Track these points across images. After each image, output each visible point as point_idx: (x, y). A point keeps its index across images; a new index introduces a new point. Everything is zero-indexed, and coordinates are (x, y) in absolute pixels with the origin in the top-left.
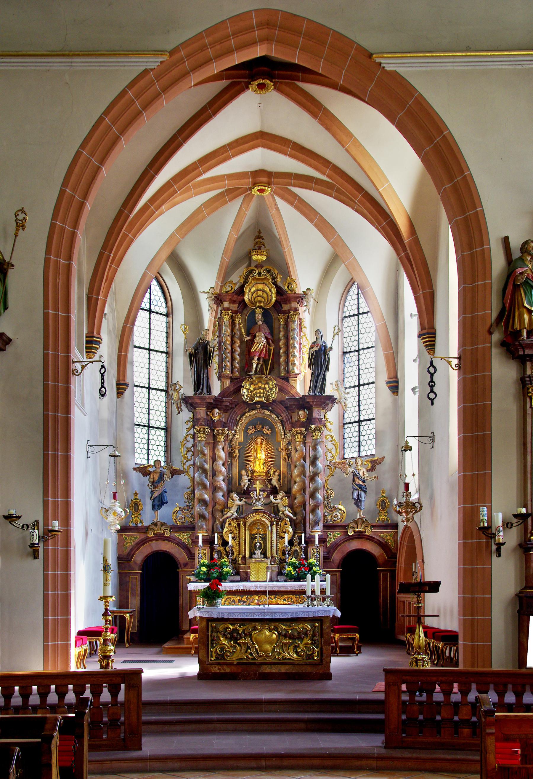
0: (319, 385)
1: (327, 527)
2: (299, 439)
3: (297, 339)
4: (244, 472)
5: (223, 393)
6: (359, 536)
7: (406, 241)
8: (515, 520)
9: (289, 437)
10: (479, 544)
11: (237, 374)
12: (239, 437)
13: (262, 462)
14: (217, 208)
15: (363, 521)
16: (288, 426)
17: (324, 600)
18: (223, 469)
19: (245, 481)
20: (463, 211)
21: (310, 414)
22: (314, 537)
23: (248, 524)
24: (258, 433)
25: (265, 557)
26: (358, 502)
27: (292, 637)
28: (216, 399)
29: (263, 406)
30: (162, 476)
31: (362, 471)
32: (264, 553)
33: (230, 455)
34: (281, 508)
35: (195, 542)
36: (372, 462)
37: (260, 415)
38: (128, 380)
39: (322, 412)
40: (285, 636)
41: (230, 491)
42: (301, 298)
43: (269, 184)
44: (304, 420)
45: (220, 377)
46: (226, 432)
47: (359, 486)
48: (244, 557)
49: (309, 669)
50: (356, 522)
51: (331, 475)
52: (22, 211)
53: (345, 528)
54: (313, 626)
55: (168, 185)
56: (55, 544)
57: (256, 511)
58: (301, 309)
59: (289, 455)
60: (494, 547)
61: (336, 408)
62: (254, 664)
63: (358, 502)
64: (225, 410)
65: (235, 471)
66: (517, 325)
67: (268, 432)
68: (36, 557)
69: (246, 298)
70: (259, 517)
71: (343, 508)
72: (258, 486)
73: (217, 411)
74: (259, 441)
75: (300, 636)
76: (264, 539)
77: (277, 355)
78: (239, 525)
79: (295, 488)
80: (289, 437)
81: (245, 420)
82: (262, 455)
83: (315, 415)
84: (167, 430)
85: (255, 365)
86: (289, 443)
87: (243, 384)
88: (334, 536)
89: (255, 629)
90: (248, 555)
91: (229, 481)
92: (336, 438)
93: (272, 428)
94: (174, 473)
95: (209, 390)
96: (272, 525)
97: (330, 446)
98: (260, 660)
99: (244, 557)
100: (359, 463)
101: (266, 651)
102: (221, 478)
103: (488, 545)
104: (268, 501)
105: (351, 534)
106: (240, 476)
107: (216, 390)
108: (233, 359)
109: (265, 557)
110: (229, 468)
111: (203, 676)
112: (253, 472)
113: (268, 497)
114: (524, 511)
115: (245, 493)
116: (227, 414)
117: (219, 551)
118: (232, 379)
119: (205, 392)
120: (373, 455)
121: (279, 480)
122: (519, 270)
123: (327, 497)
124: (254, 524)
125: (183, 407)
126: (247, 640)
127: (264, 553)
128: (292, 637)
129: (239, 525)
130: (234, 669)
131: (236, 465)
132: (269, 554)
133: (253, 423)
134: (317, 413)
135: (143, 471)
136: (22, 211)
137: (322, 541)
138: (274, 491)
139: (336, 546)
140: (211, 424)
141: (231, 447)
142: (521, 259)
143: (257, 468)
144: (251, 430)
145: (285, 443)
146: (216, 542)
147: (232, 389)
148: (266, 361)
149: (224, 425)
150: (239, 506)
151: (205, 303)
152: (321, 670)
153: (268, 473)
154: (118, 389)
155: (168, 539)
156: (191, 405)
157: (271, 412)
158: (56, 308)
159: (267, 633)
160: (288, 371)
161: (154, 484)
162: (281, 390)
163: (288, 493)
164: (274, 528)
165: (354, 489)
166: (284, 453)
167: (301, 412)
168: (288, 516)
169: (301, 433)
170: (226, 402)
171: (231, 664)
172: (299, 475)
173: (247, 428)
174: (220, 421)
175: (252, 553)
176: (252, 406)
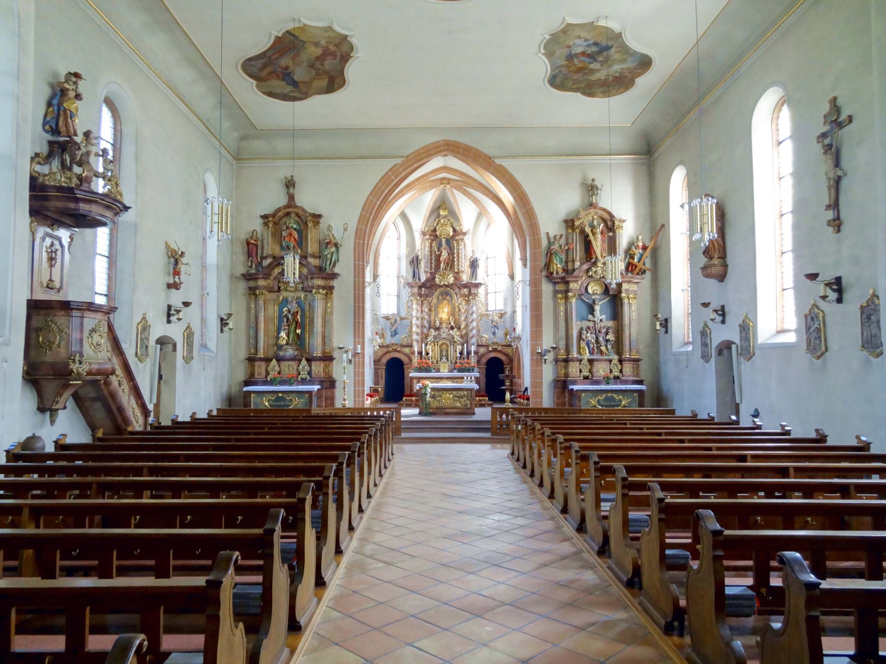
0: (474, 276)
1: (479, 346)
2: (464, 302)
3: (463, 253)
4: (437, 319)
5: (427, 280)
6: (495, 350)
7: (512, 218)
8: (551, 350)
9: (459, 301)
10: (537, 359)
11: (433, 271)
12: (435, 301)
13: (446, 313)
14: (423, 193)
15: (496, 343)
16: (459, 296)
17: (471, 382)
18: (427, 317)
19: (438, 324)
20: (530, 221)
21: (470, 291)
22: (471, 351)
23: (439, 345)
24: (444, 299)
25: (448, 360)
26: (494, 334)
27: (458, 397)
28: (423, 283)
29: (447, 286)
30: (396, 321)
31: (496, 318)
32: (447, 359)
33: (430, 310)
34: (455, 337)
35: (413, 353)
36: (501, 314)
37: (445, 290)
38: (378, 274)
39: (476, 290)
40: (456, 397)
41: (430, 328)
42: (465, 234)
43: (449, 183)
44: (467, 293)
45: (426, 272)
46: (428, 299)
47: (495, 325)
48: (437, 361)
49: (465, 411)
50: (493, 343)
51: (481, 320)
52: (346, 224)
53: (487, 346)
54: (468, 393)
55: (401, 191)
56: (359, 358)
57: (443, 339)
58: (465, 238)
59: (460, 310)
60: (543, 361)
61: (483, 287)
62: (442, 408)
63: (494, 334)
64: (427, 288)
65: (432, 317)
66: (551, 270)
67: (449, 299)
68: (351, 364)
69: (438, 233)
70: (444, 342)
71: (487, 337)
72: (444, 326)
73: (423, 289)
74: (444, 303)
75: (462, 397)
76: (447, 352)
77: (453, 261)
78: (434, 345)
79: (462, 327)
80: (459, 301)
81: (437, 293)
82: (446, 310)
83: (472, 291)
84: (398, 296)
85: (442, 266)
86: (459, 304)
87: (436, 276)
88: (482, 350)
89: (443, 394)
90: (439, 359)
91: (429, 322)
92: (483, 301)
93: (451, 296)
94: (402, 319)
95: (419, 279)
96: (451, 345)
97: (480, 305)
98: (445, 407)
99: (437, 361)
100: (495, 314)
101: (448, 403)
102: (426, 321)
103: (541, 359)
104: (449, 333)
105: (490, 349)
106: (435, 321)
107: (423, 278)
108: (431, 263)
109: (448, 360)
110: (430, 316)
111: (420, 414)
112: (442, 318)
113: (449, 331)
114: (554, 346)
115: (437, 329)
116: (428, 290)
117: (425, 358)
118: (431, 273)
119: (417, 280)
120: (502, 310)
121: (455, 322)
122: (552, 247)
123: (478, 331)
124: (442, 344)
125: (407, 286)
126: (439, 398)
127: (447, 359)
128: (458, 397)
129: (434, 345)
130: (435, 411)
131: (433, 314)
132: (449, 359)
133: (442, 294)
134: (473, 290)
135: (387, 318)
136: (346, 224)
137: (476, 353)
138: (452, 328)
139: (483, 355)
140: (420, 295)
141: (430, 305)
142: (554, 242)
143: (444, 317)
144: (441, 298)
145: (457, 304)
146: (423, 354)
147: (431, 278)
148: (448, 264)
149: (427, 296)
150: (434, 336)
151: (418, 237)
152: (471, 411)
153: (449, 318)
154: (374, 278)
155: (399, 352)
156: (411, 286)
157: (451, 288)
158: (359, 261)
159: (448, 395)
160: (458, 269)
161: (392, 325)
162: (456, 278)
163: (459, 328)
164: (452, 346)
165: (492, 327)
166: (457, 309)
167: (465, 290)
168: (459, 341)
169: (465, 300)
170: (428, 284)
171: (432, 408)
172: (465, 320)
173: (438, 297)
174: (425, 294)
175: (441, 359)
176: (441, 286)
